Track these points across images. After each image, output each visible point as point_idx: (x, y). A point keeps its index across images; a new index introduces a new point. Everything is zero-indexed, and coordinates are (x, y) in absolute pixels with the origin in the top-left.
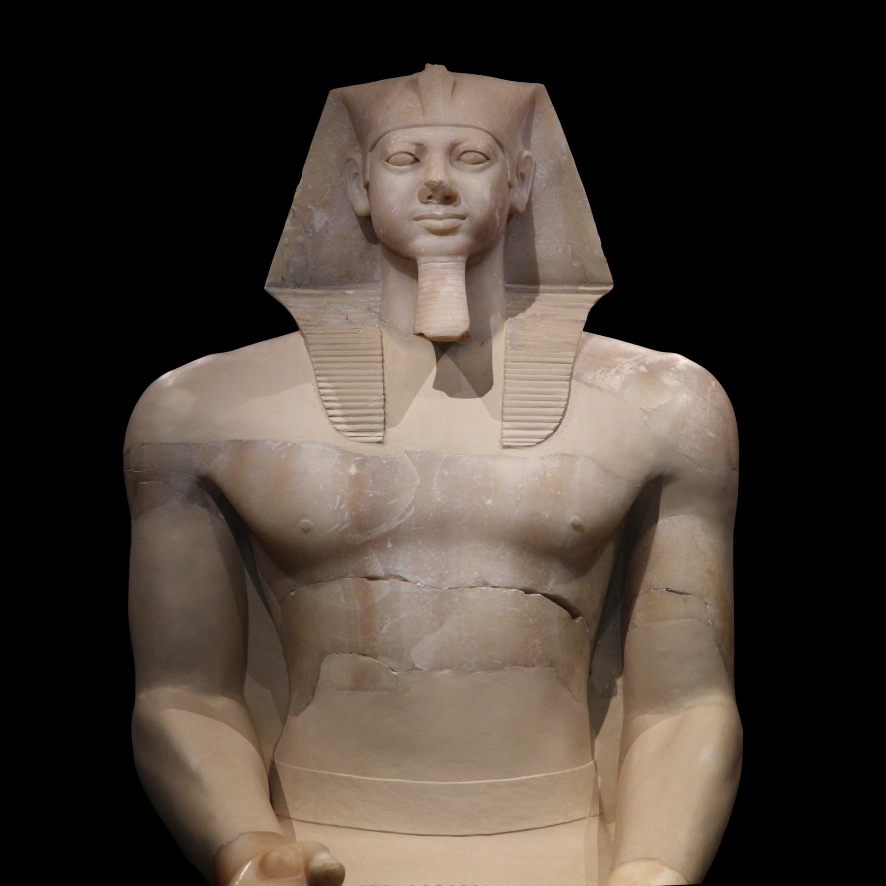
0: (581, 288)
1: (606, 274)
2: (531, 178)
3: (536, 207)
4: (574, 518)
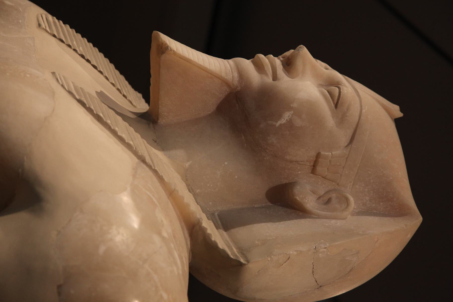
2: (329, 214)
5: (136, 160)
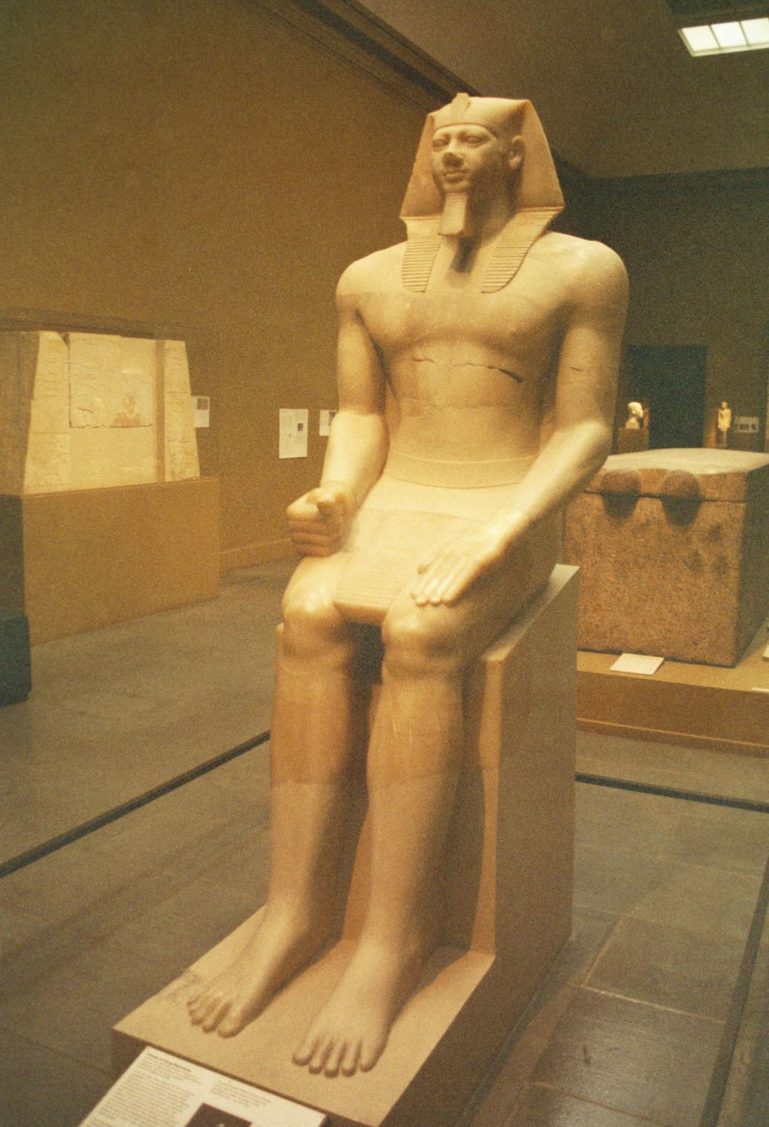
0: (549, 208)
1: (561, 200)
3: (525, 168)
4: (514, 330)
5: (527, 259)
